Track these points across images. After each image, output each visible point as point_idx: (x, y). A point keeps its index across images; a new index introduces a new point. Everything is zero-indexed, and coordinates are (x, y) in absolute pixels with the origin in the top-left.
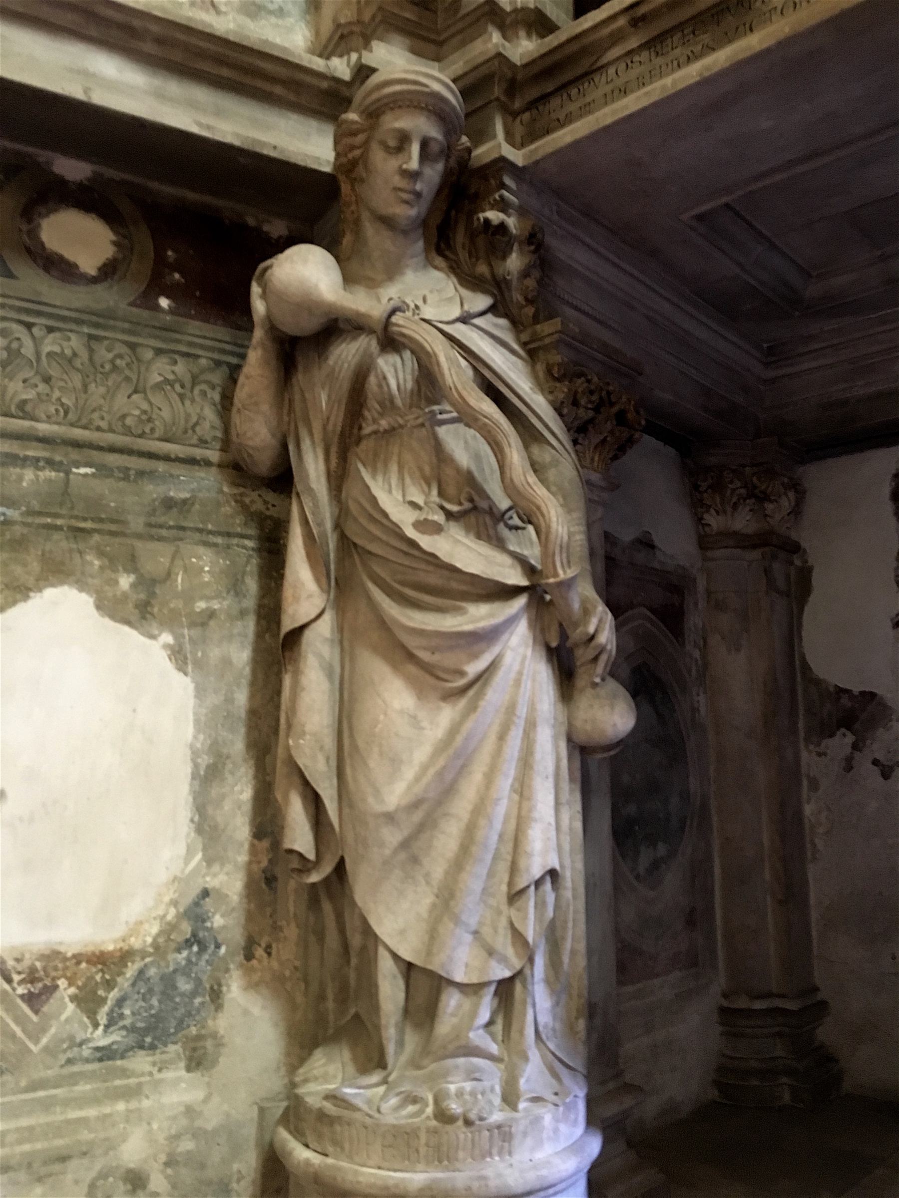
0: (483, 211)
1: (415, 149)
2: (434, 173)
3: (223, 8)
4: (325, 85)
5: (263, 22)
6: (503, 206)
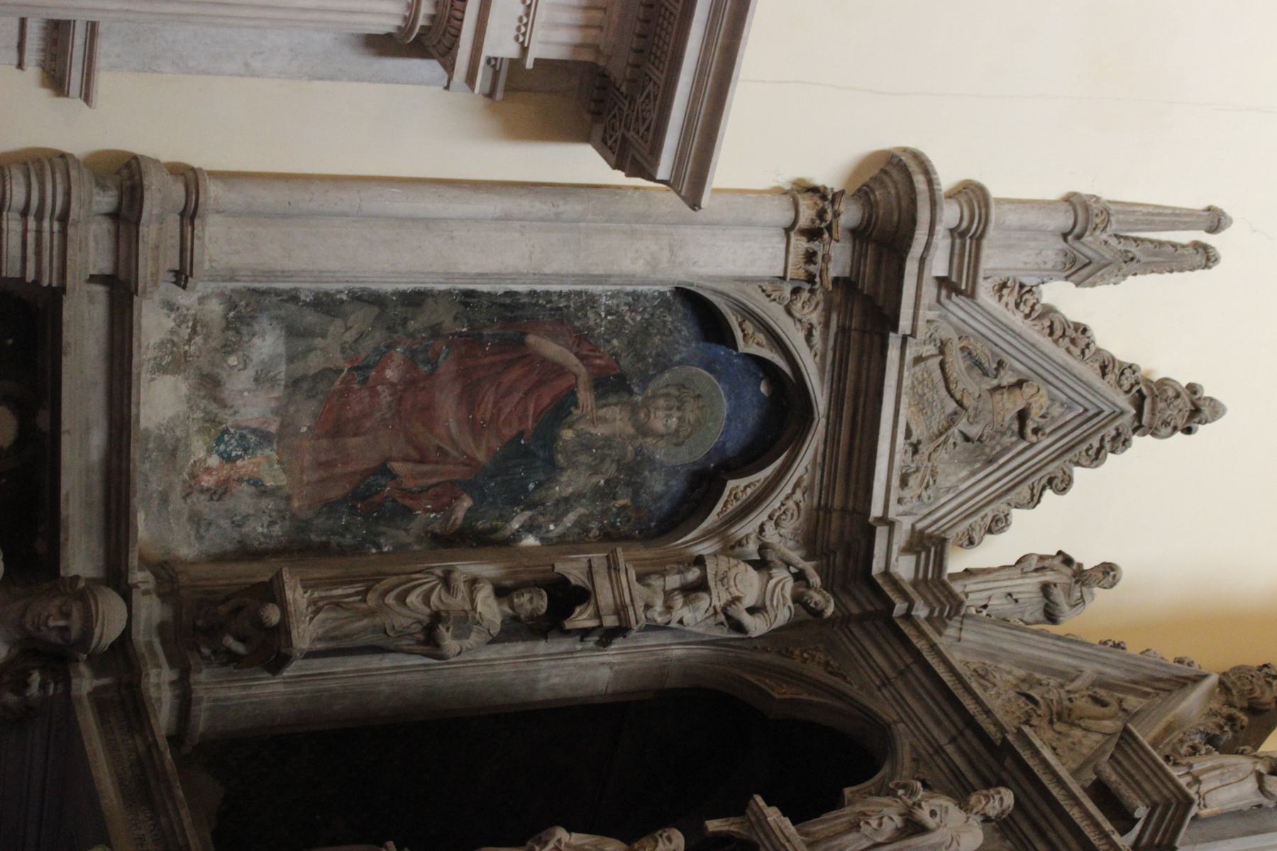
0: (41, 673)
1: (62, 623)
2: (54, 637)
3: (189, 501)
4: (123, 568)
5: (189, 527)
6: (43, 686)
